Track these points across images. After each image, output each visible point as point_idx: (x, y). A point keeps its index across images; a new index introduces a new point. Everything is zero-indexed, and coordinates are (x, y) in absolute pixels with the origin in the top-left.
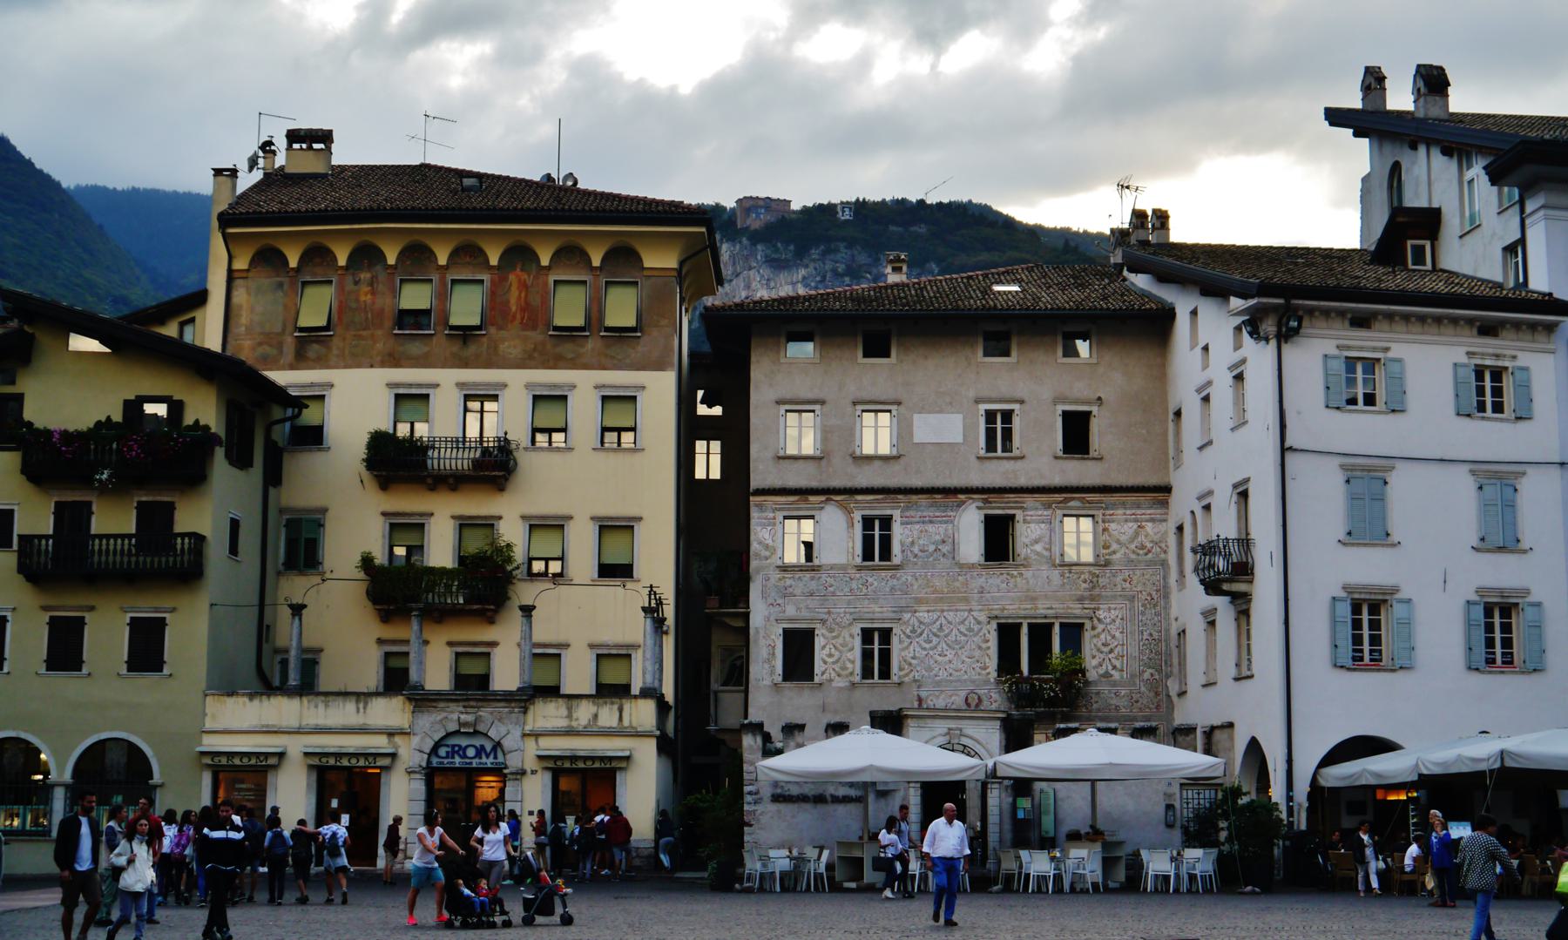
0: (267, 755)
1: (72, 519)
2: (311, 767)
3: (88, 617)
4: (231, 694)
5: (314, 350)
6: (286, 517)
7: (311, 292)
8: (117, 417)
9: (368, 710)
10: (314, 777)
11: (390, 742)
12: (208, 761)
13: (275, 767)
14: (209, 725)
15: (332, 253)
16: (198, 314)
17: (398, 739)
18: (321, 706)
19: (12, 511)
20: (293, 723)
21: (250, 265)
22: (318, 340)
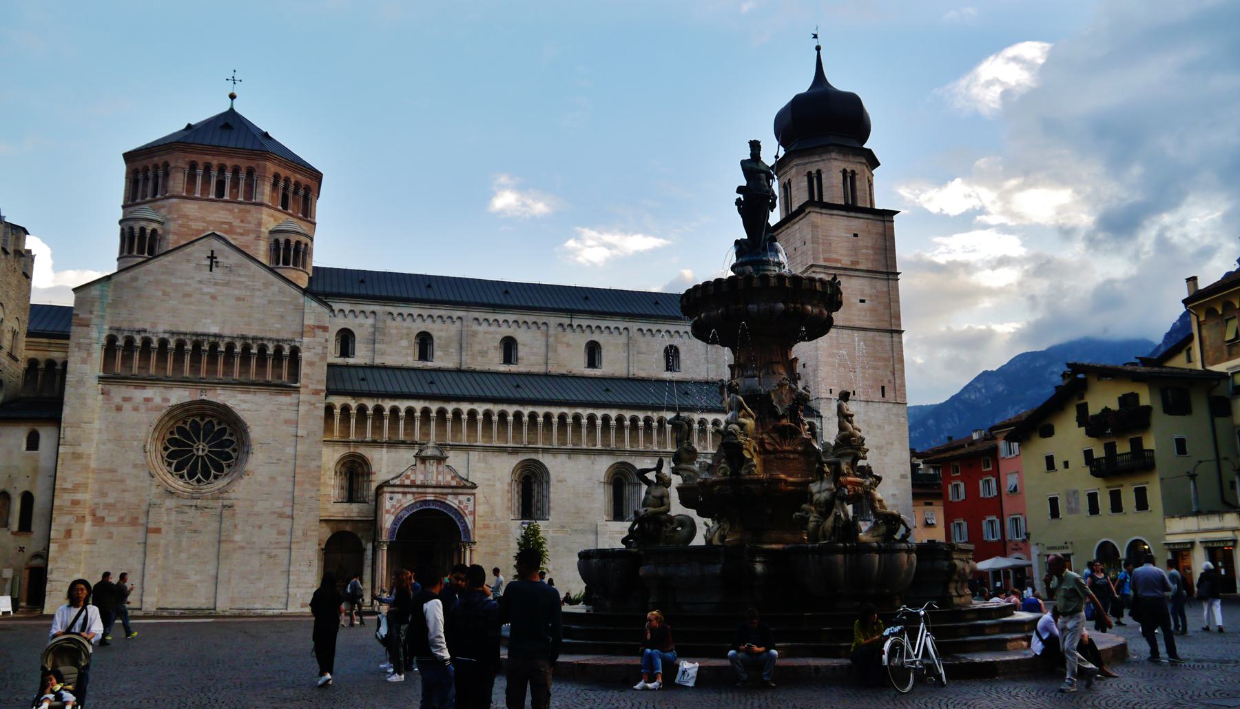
0: (1186, 543)
1: (1110, 448)
2: (1205, 548)
3: (1121, 489)
4: (1173, 517)
5: (1235, 349)
6: (1237, 429)
7: (1230, 323)
8: (1114, 406)
9: (1224, 520)
10: (1207, 551)
11: (1234, 534)
12: (1166, 547)
13: (1188, 550)
14: (1168, 531)
15: (1232, 303)
16: (1191, 345)
17: (1236, 533)
18: (1206, 519)
19: (1092, 450)
20: (1195, 528)
21: (1206, 317)
22: (1236, 345)
